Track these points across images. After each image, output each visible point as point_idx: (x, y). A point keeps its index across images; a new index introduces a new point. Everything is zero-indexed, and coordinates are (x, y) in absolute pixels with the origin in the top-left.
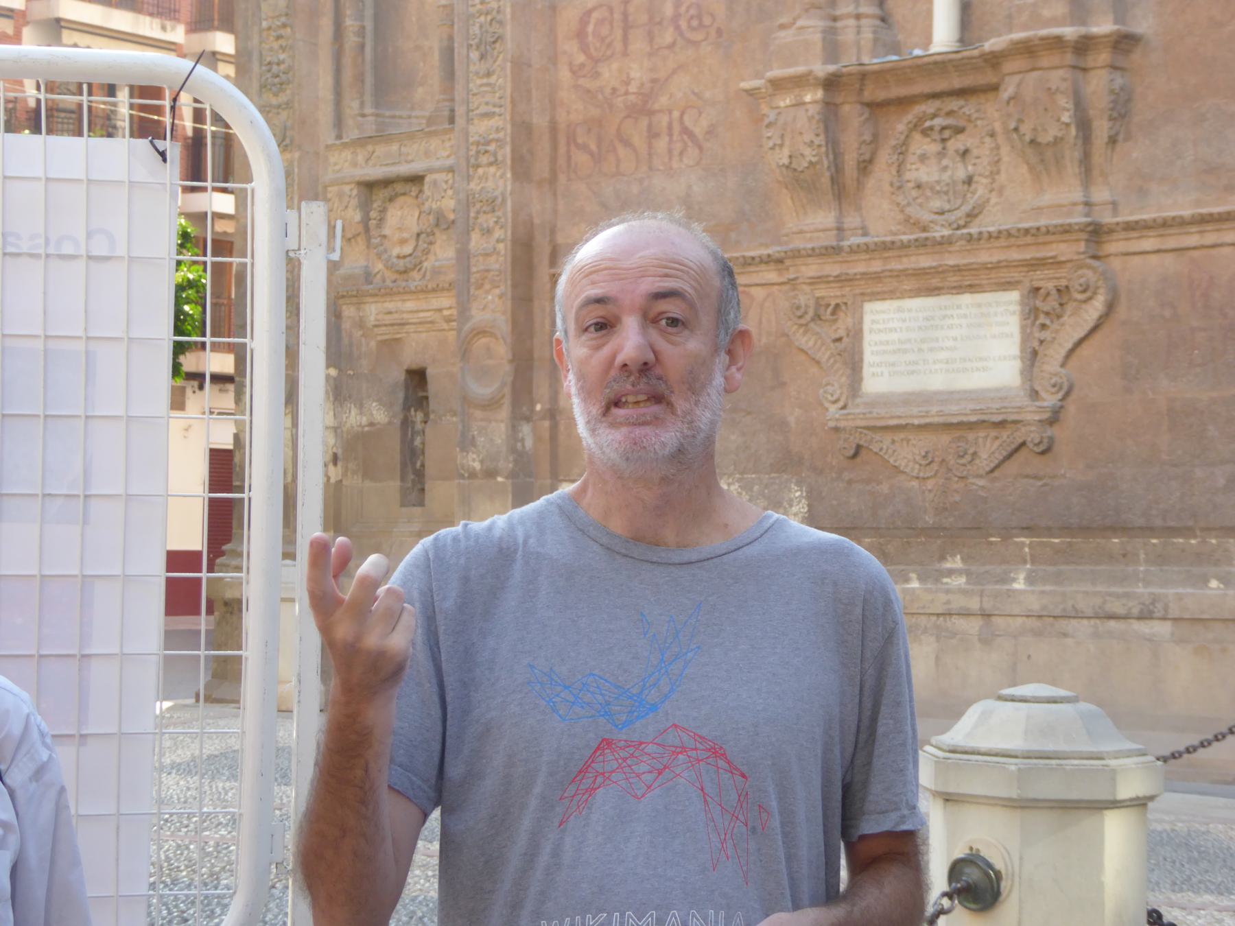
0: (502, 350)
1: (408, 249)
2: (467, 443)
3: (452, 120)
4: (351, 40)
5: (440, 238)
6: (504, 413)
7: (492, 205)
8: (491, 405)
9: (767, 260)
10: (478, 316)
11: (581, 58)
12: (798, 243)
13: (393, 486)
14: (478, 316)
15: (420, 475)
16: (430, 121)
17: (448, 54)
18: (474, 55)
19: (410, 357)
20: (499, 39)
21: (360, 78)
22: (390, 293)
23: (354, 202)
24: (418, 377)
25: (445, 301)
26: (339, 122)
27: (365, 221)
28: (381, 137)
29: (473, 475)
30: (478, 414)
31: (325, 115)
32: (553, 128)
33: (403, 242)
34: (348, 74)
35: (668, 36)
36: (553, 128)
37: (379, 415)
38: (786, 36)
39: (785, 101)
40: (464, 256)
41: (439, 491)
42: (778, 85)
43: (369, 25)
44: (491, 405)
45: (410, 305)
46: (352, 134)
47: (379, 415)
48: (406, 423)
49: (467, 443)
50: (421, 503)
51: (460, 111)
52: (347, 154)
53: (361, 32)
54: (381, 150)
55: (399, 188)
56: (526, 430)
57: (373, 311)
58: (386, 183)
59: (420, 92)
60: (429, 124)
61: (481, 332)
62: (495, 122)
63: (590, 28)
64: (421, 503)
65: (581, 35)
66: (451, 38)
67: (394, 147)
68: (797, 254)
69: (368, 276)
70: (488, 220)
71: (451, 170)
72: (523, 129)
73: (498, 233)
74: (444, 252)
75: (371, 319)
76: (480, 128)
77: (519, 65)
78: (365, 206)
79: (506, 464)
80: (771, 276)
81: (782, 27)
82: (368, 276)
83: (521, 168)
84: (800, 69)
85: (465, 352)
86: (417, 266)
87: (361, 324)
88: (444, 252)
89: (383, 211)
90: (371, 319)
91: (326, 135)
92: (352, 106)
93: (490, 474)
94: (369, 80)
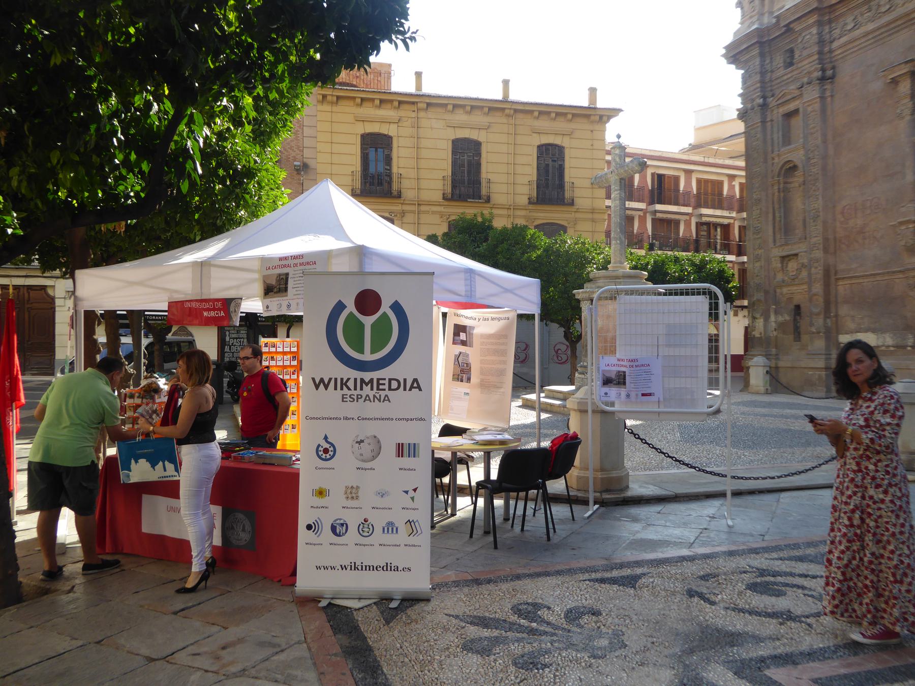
0: (821, 300)
1: (794, 273)
2: (811, 325)
3: (805, 239)
4: (778, 219)
5: (803, 270)
6: (822, 316)
7: (817, 261)
8: (818, 314)
9: (900, 272)
10: (814, 290)
11: (843, 219)
12: (909, 267)
13: (791, 337)
14: (814, 290)
15: (799, 333)
16: (800, 239)
17: (804, 221)
18: (812, 221)
19: (795, 302)
20: (818, 216)
21: (780, 229)
22: (789, 285)
23: (779, 262)
24: (798, 307)
25: (805, 287)
26: (775, 241)
27: (782, 266)
28: (786, 244)
29: (813, 333)
30: (815, 317)
31: (771, 239)
32: (835, 238)
33: (793, 271)
34: (777, 229)
35: (868, 212)
36: (835, 238)
37: (787, 317)
38: (903, 210)
39: (903, 228)
40: (810, 275)
41: (805, 338)
42: (901, 223)
43: (782, 214)
44: (818, 314)
45: (795, 288)
46: (778, 244)
47: (787, 317)
48: (795, 320)
49: (811, 325)
50: (799, 341)
51: (808, 236)
52: (777, 249)
53: (780, 217)
54: (786, 248)
55: (791, 257)
56: (828, 320)
57: (785, 290)
58: (788, 256)
59: (797, 231)
60: (800, 240)
61: (815, 295)
62: (818, 238)
63: (845, 211)
64: (799, 341)
65: (842, 213)
66: (805, 217)
67: (790, 247)
68: (909, 270)
69: (783, 281)
70: (816, 265)
71: (805, 252)
72: (826, 240)
73: (819, 268)
74: (804, 274)
75: (784, 293)
76: (814, 240)
77: (825, 223)
78: (782, 263)
79: (823, 330)
80: (901, 276)
81: (903, 207)
82: (783, 281)
83: (826, 250)
84: (907, 219)
85: (810, 300)
86: (797, 278)
87: (782, 294)
88: (804, 274)
89: (787, 264)
90: (784, 293)
91: (771, 244)
92: (778, 236)
93: (819, 333)
94: (783, 230)
